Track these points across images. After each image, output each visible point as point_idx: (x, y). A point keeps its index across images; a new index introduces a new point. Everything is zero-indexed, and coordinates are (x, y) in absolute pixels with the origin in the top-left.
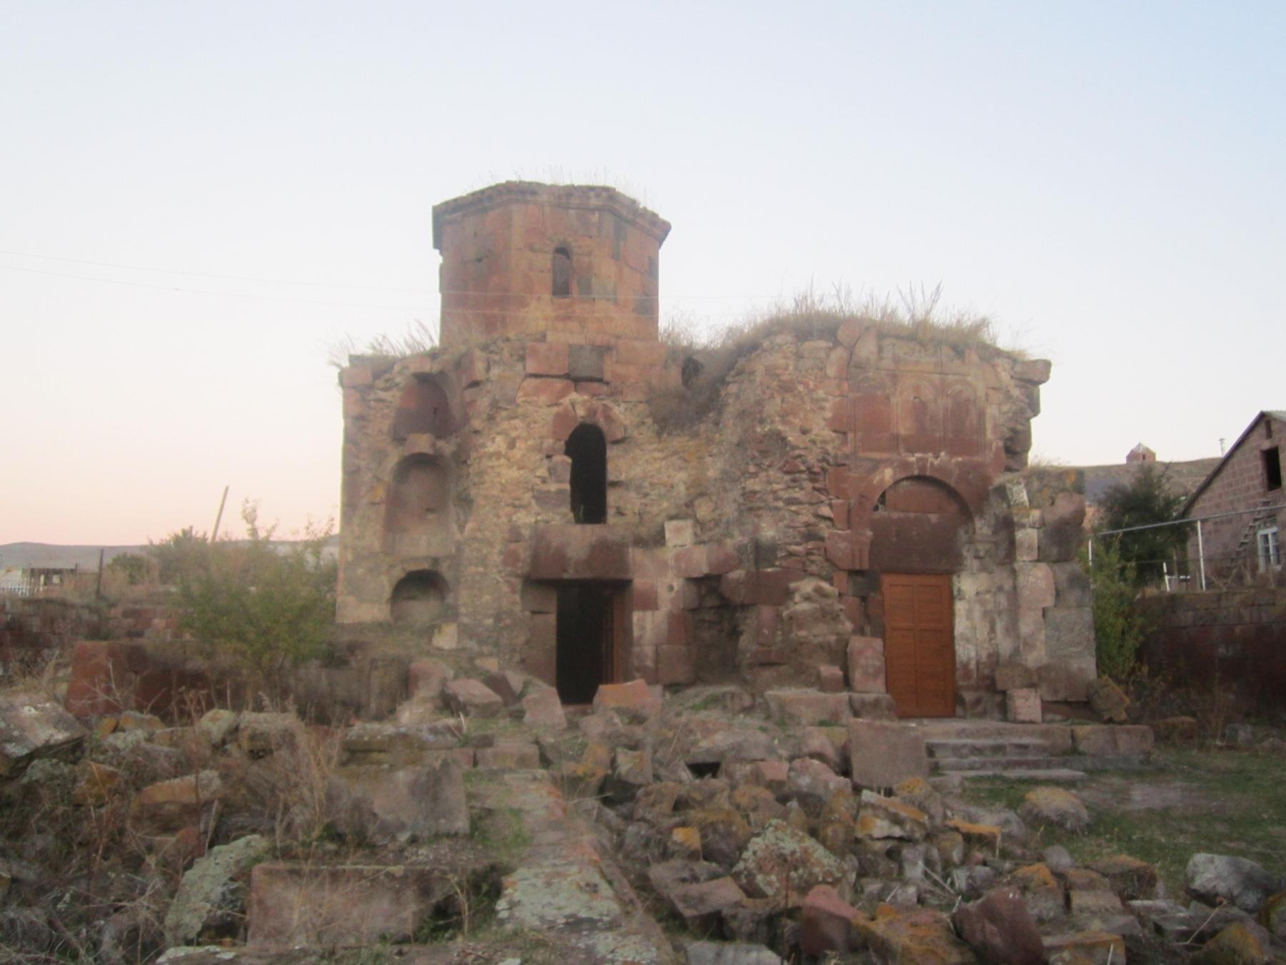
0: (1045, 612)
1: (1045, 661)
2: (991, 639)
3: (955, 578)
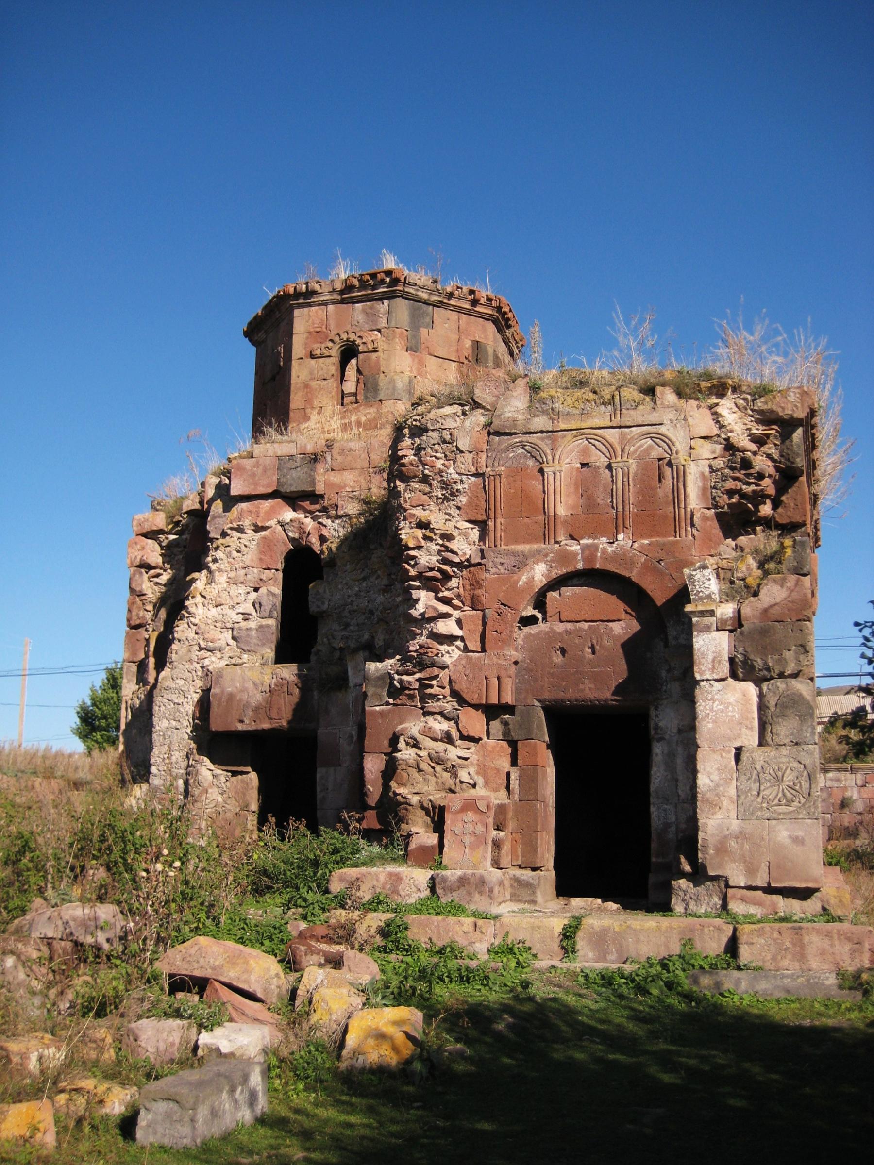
0: (739, 751)
1: (735, 825)
3: (652, 712)
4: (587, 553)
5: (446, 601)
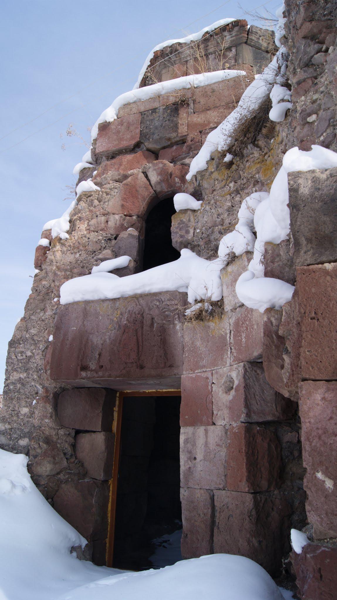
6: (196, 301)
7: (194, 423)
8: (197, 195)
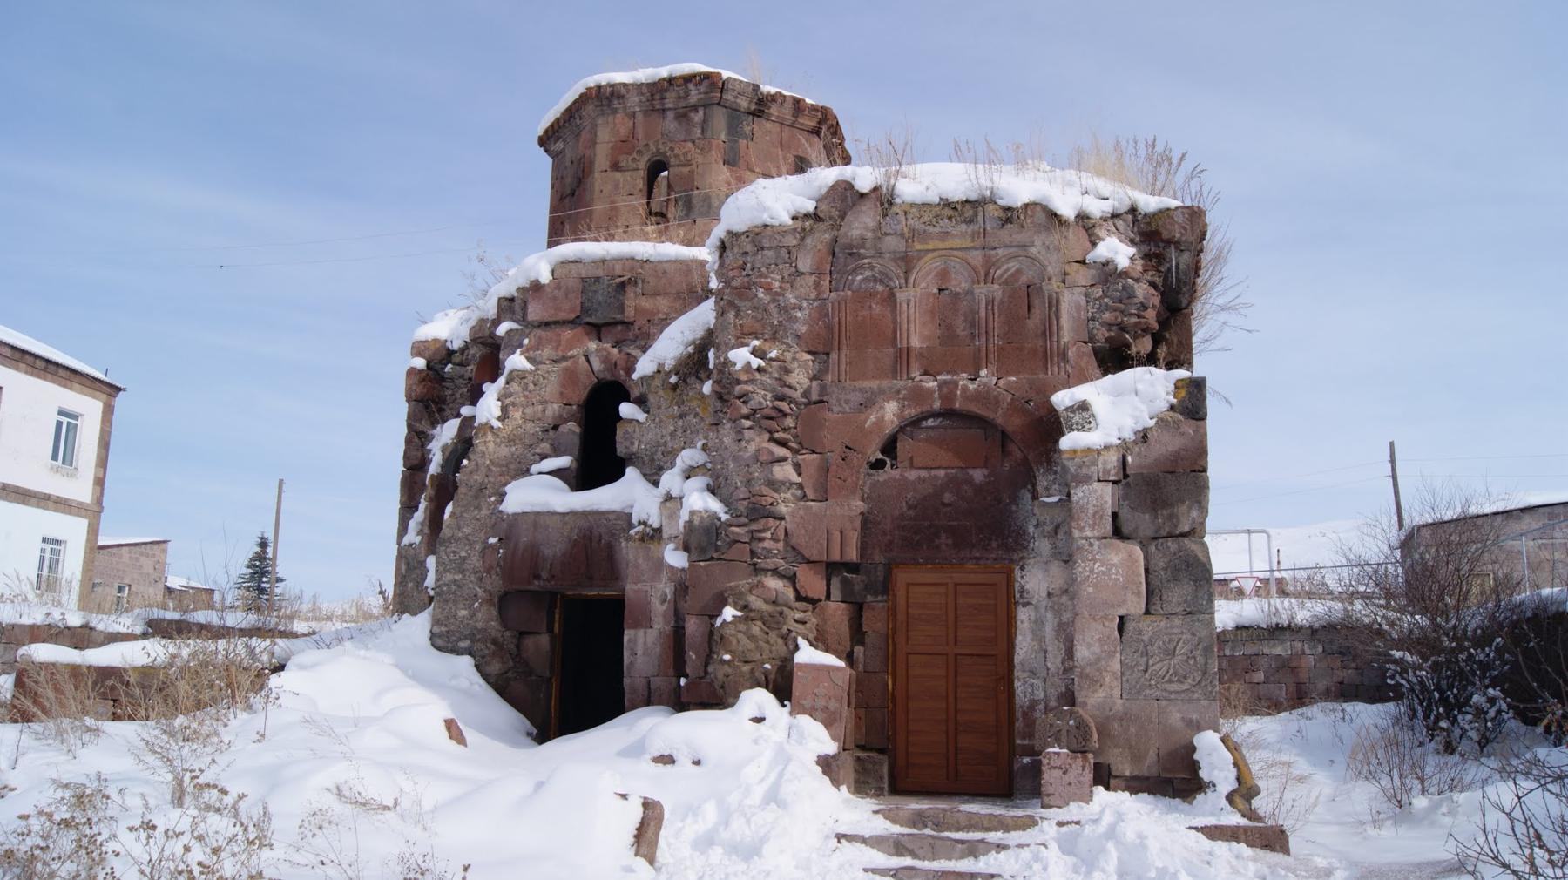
2: (1066, 671)
4: (945, 390)
5: (783, 443)
6: (640, 523)
7: (636, 625)
8: (641, 402)
